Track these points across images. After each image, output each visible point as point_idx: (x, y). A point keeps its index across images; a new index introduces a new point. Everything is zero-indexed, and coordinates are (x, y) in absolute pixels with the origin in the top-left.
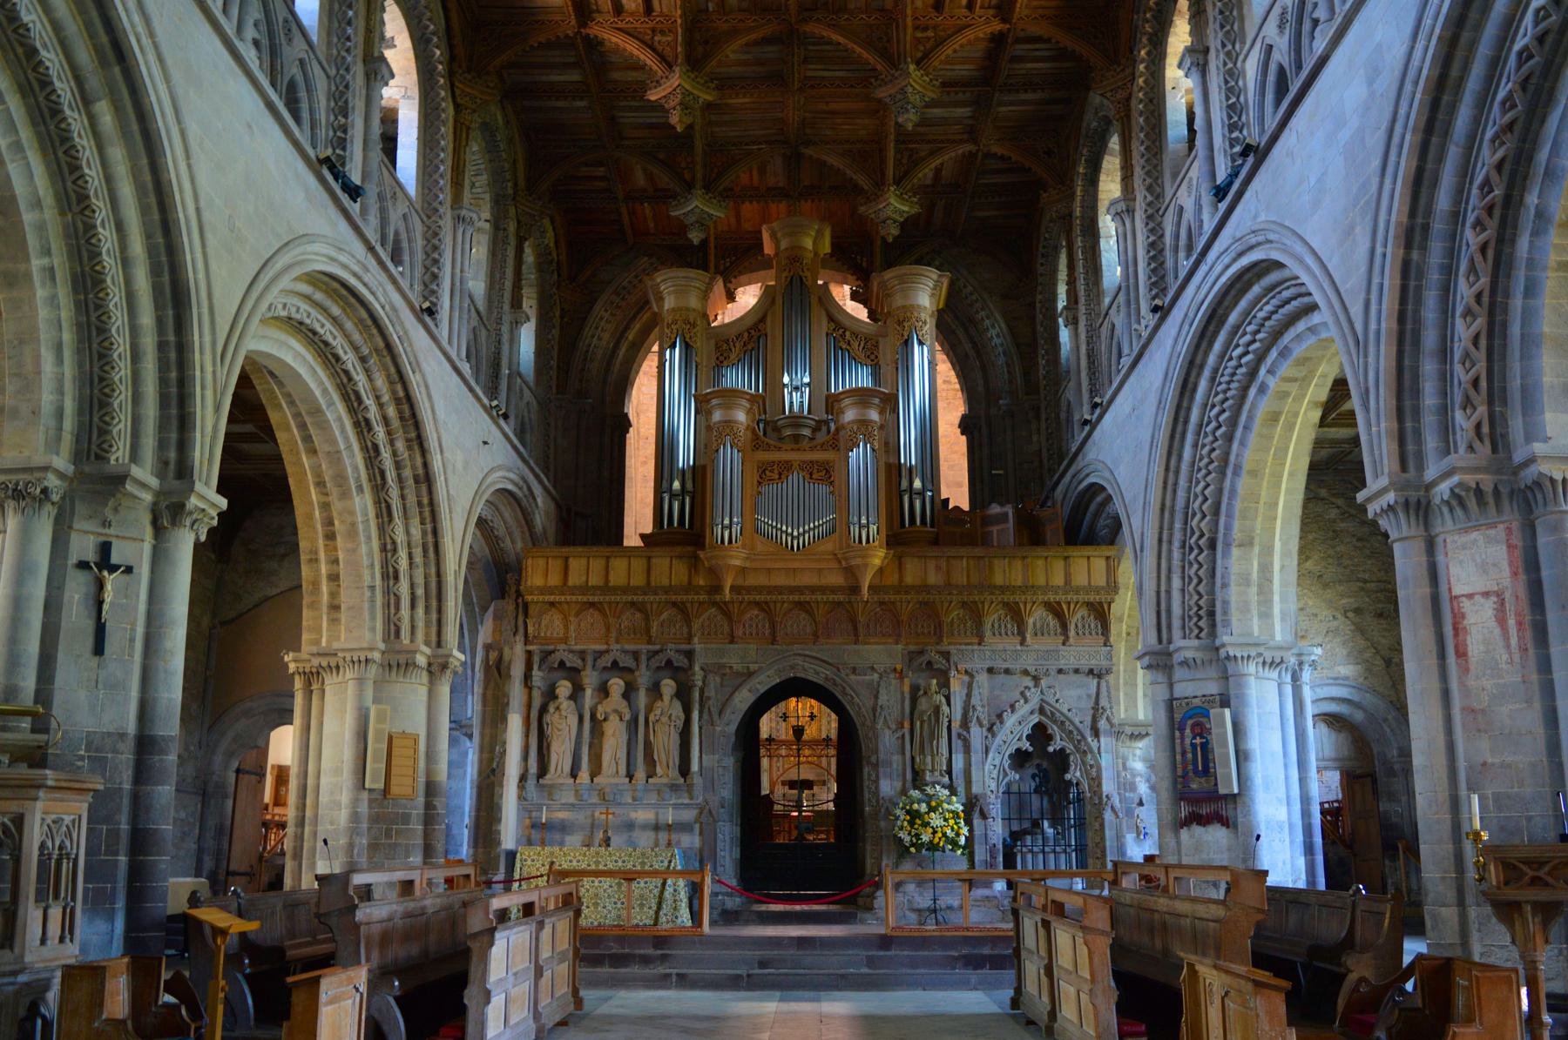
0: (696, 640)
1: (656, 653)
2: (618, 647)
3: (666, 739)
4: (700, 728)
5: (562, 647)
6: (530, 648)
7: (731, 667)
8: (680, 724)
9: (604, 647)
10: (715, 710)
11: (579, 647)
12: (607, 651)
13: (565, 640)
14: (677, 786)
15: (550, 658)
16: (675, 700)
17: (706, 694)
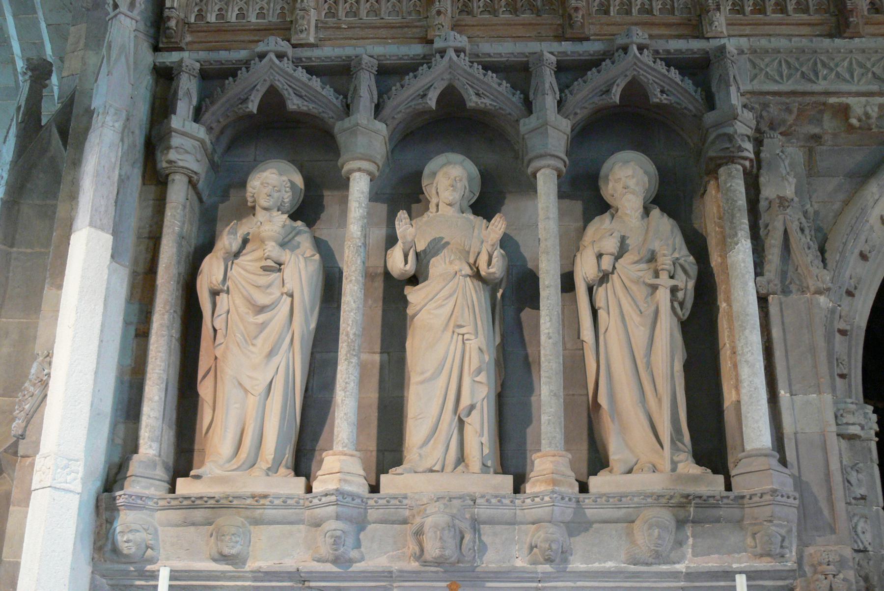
0: (720, 21)
1: (594, 63)
2: (462, 41)
3: (640, 335)
4: (763, 301)
5: (274, 43)
6: (171, 58)
7: (844, 111)
8: (687, 285)
9: (418, 49)
10: (801, 243)
11: (329, 52)
12: (427, 60)
13: (285, 29)
14: (705, 502)
15: (233, 88)
16: (656, 212)
17: (768, 192)
